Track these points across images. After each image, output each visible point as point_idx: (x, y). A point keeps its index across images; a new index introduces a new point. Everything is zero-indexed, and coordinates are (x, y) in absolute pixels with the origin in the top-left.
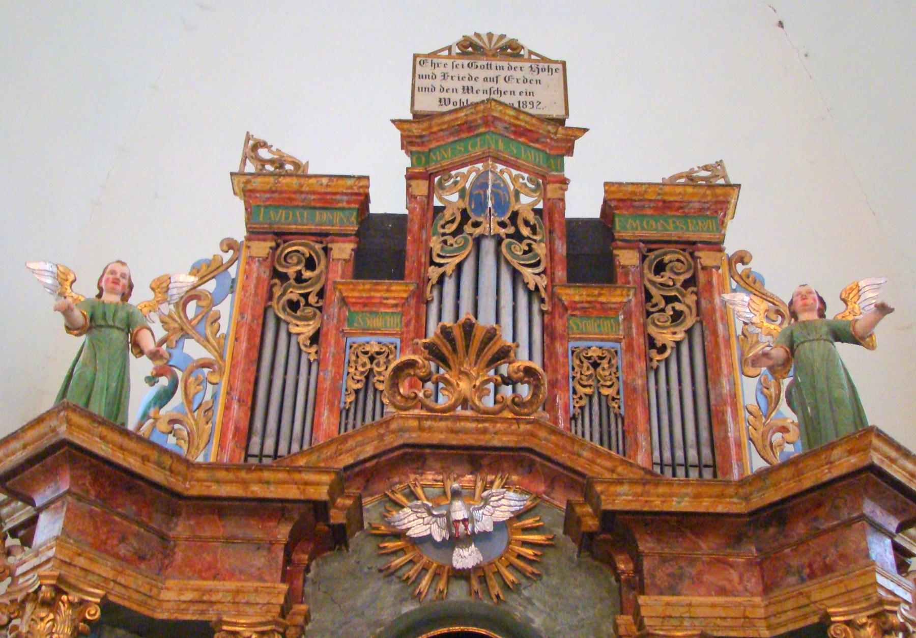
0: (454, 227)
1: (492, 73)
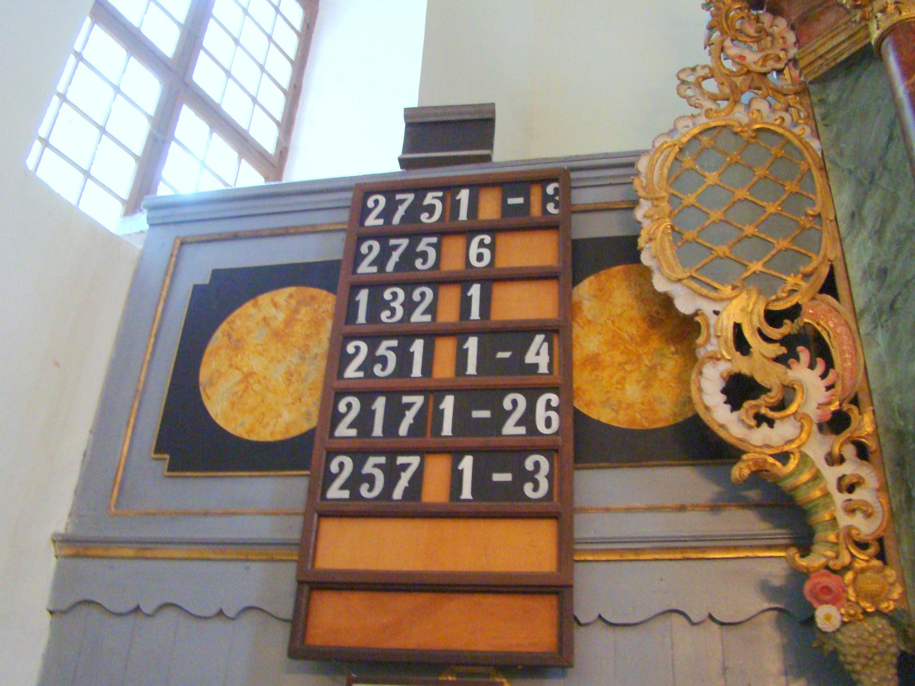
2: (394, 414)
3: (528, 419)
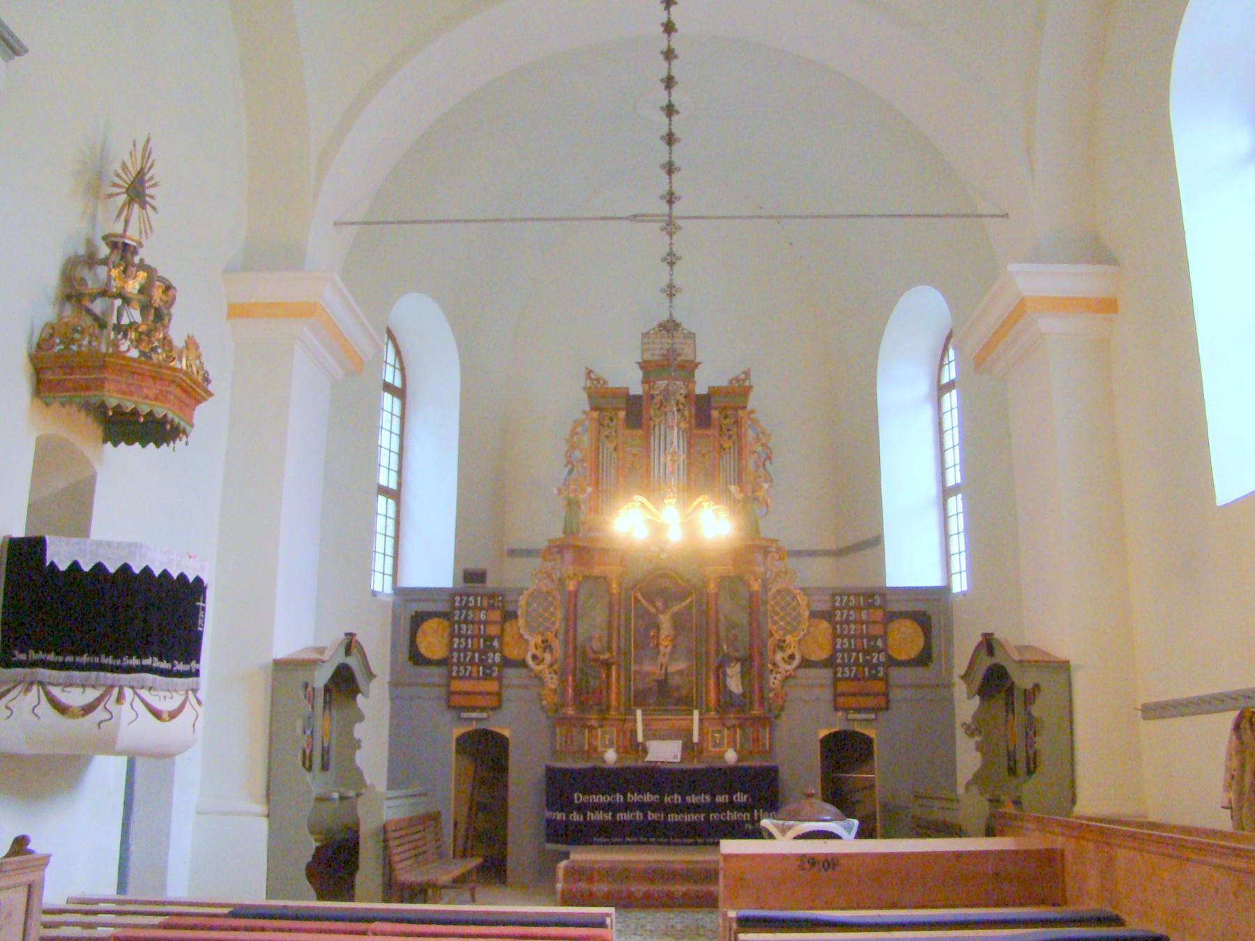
2: (465, 657)
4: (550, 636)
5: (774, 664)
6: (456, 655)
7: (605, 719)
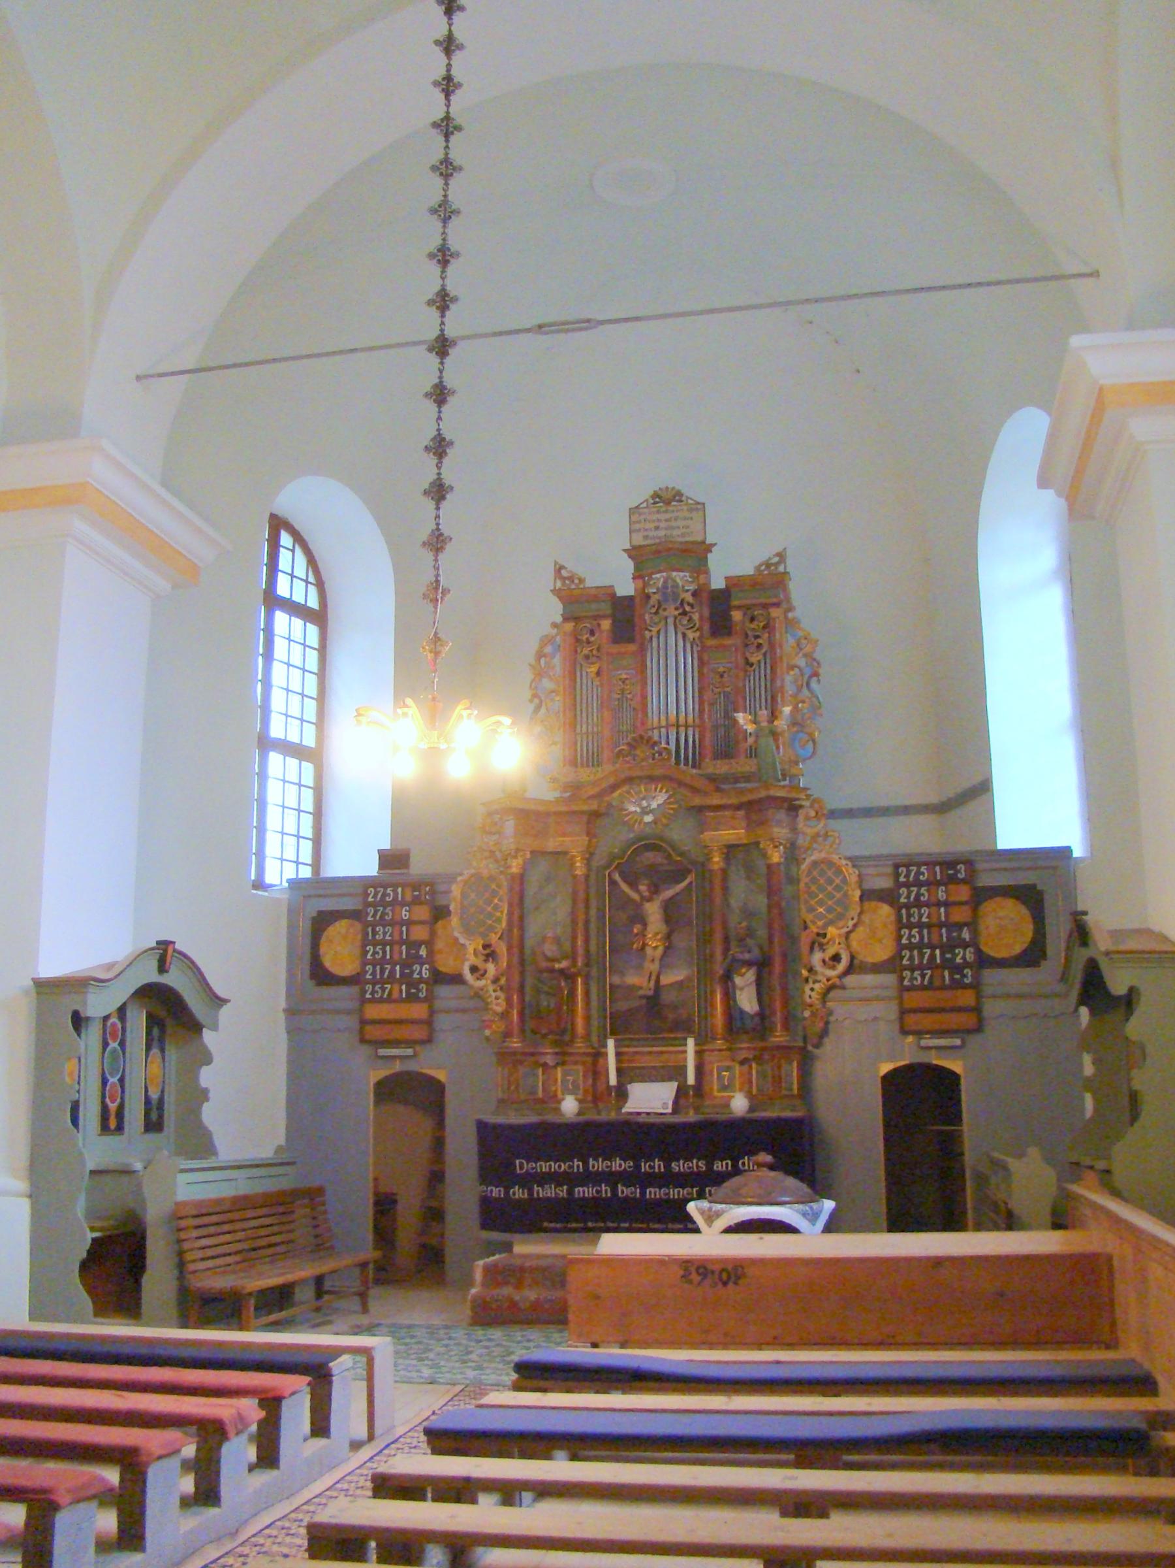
0: (654, 610)
1: (668, 516)
2: (382, 971)
3: (420, 973)
4: (493, 938)
5: (811, 970)
6: (369, 968)
7: (564, 1054)
